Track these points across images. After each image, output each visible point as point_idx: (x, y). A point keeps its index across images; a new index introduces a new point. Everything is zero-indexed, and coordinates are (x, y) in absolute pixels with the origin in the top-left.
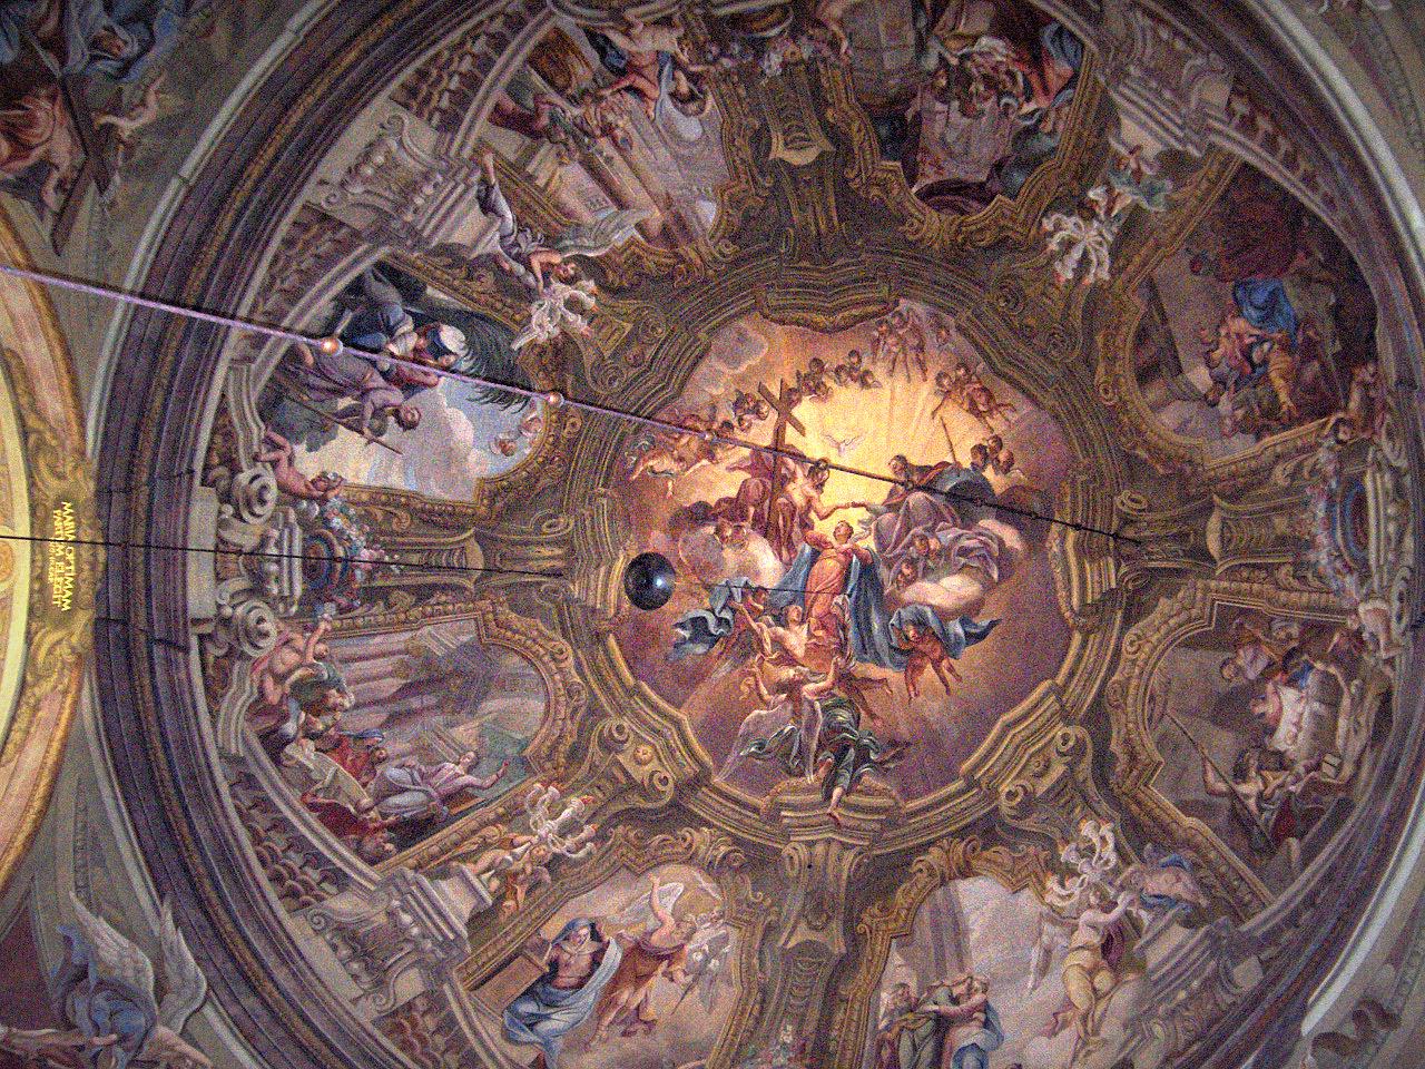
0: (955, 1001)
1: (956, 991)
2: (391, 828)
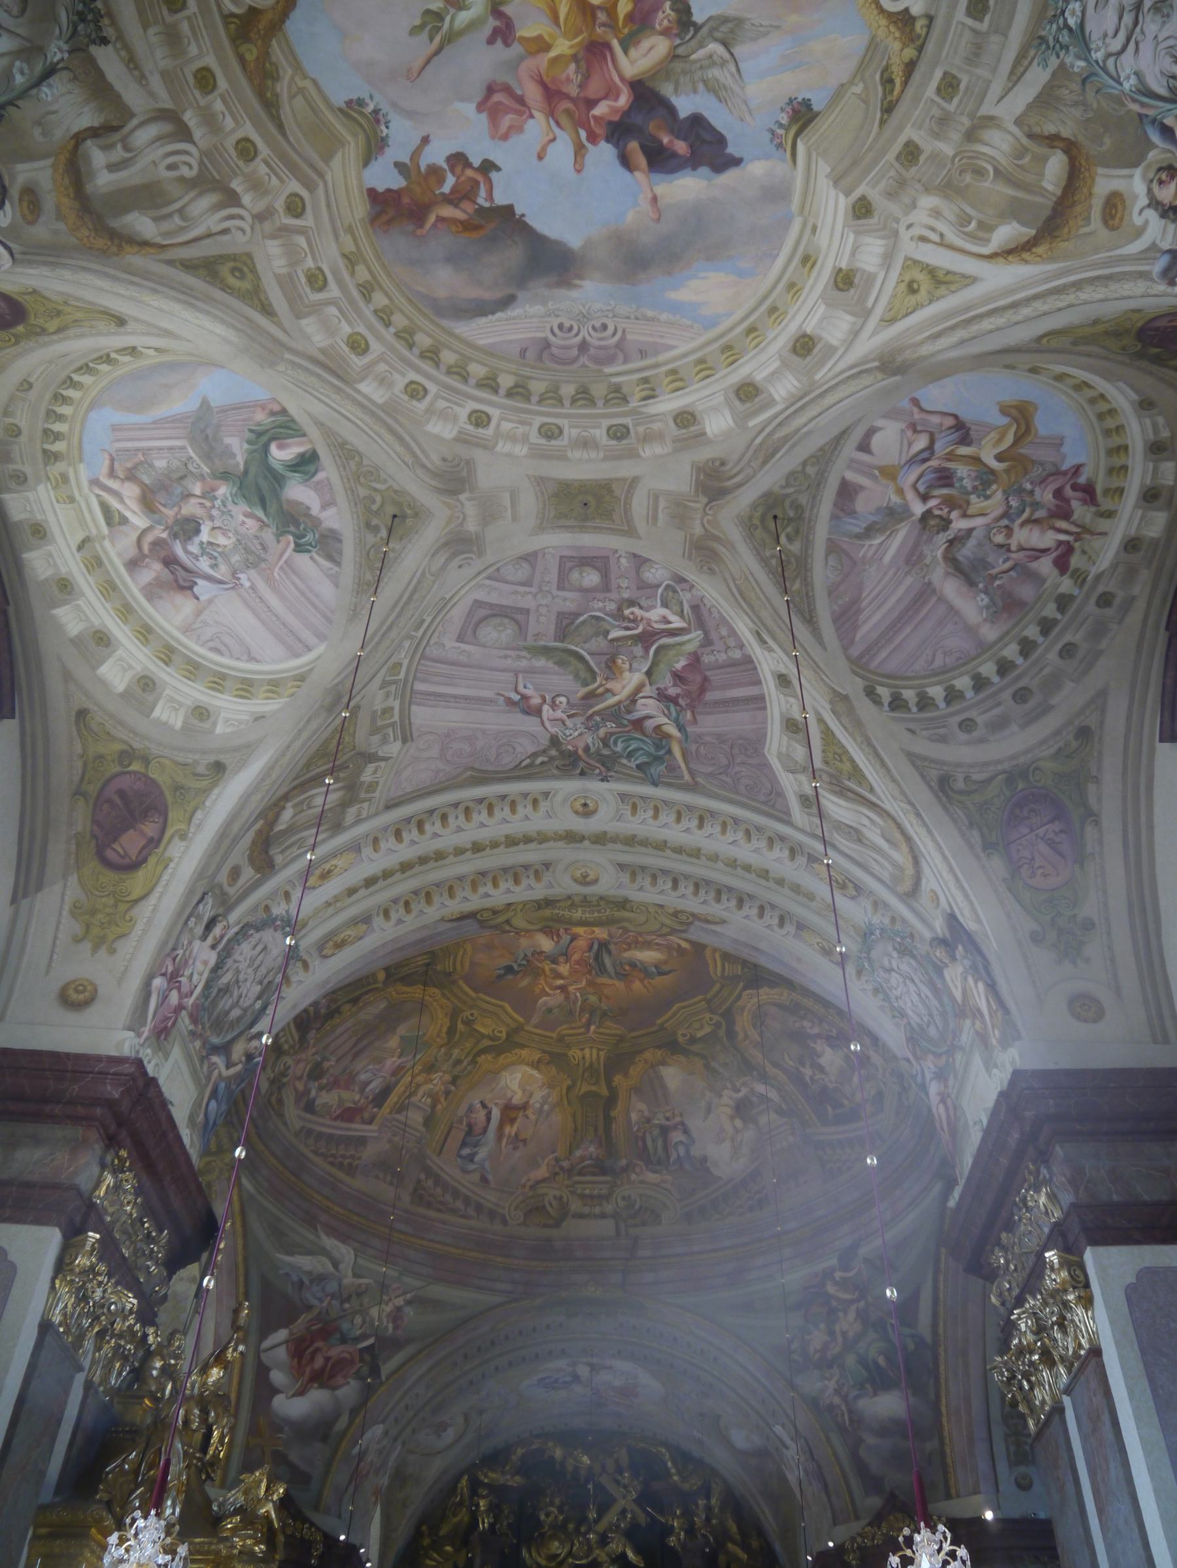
0: (668, 1119)
1: (667, 1114)
2: (372, 1101)
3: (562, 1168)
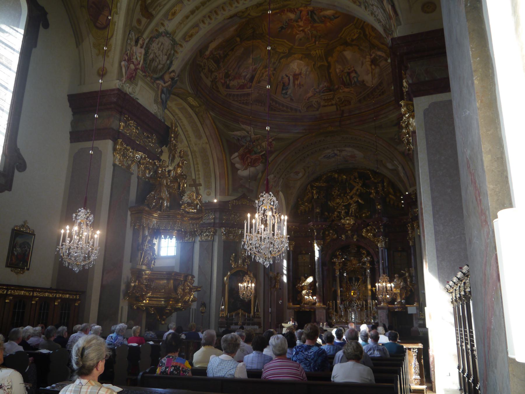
0: (349, 69)
1: (349, 68)
3: (317, 92)
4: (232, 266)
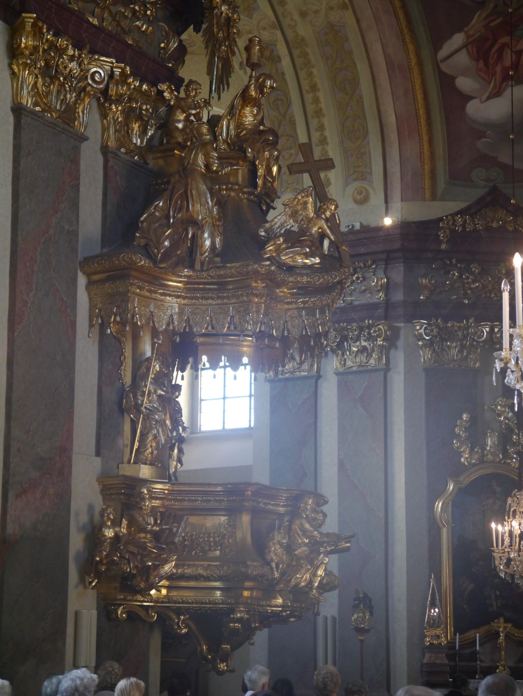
4: (462, 460)
